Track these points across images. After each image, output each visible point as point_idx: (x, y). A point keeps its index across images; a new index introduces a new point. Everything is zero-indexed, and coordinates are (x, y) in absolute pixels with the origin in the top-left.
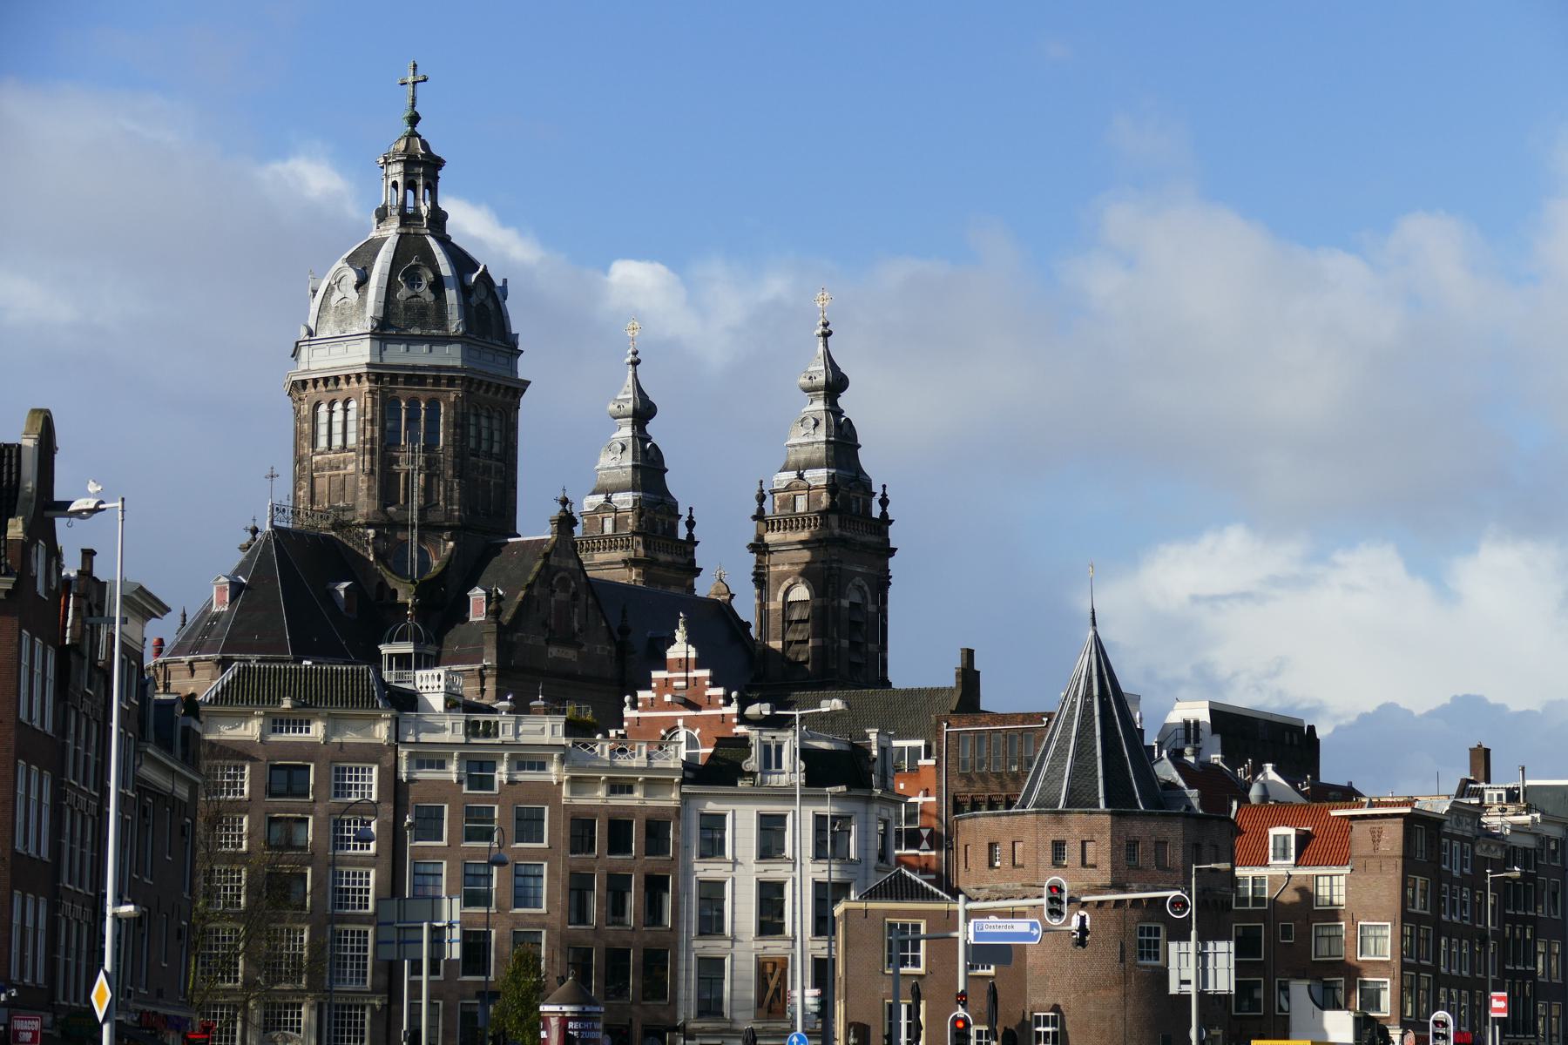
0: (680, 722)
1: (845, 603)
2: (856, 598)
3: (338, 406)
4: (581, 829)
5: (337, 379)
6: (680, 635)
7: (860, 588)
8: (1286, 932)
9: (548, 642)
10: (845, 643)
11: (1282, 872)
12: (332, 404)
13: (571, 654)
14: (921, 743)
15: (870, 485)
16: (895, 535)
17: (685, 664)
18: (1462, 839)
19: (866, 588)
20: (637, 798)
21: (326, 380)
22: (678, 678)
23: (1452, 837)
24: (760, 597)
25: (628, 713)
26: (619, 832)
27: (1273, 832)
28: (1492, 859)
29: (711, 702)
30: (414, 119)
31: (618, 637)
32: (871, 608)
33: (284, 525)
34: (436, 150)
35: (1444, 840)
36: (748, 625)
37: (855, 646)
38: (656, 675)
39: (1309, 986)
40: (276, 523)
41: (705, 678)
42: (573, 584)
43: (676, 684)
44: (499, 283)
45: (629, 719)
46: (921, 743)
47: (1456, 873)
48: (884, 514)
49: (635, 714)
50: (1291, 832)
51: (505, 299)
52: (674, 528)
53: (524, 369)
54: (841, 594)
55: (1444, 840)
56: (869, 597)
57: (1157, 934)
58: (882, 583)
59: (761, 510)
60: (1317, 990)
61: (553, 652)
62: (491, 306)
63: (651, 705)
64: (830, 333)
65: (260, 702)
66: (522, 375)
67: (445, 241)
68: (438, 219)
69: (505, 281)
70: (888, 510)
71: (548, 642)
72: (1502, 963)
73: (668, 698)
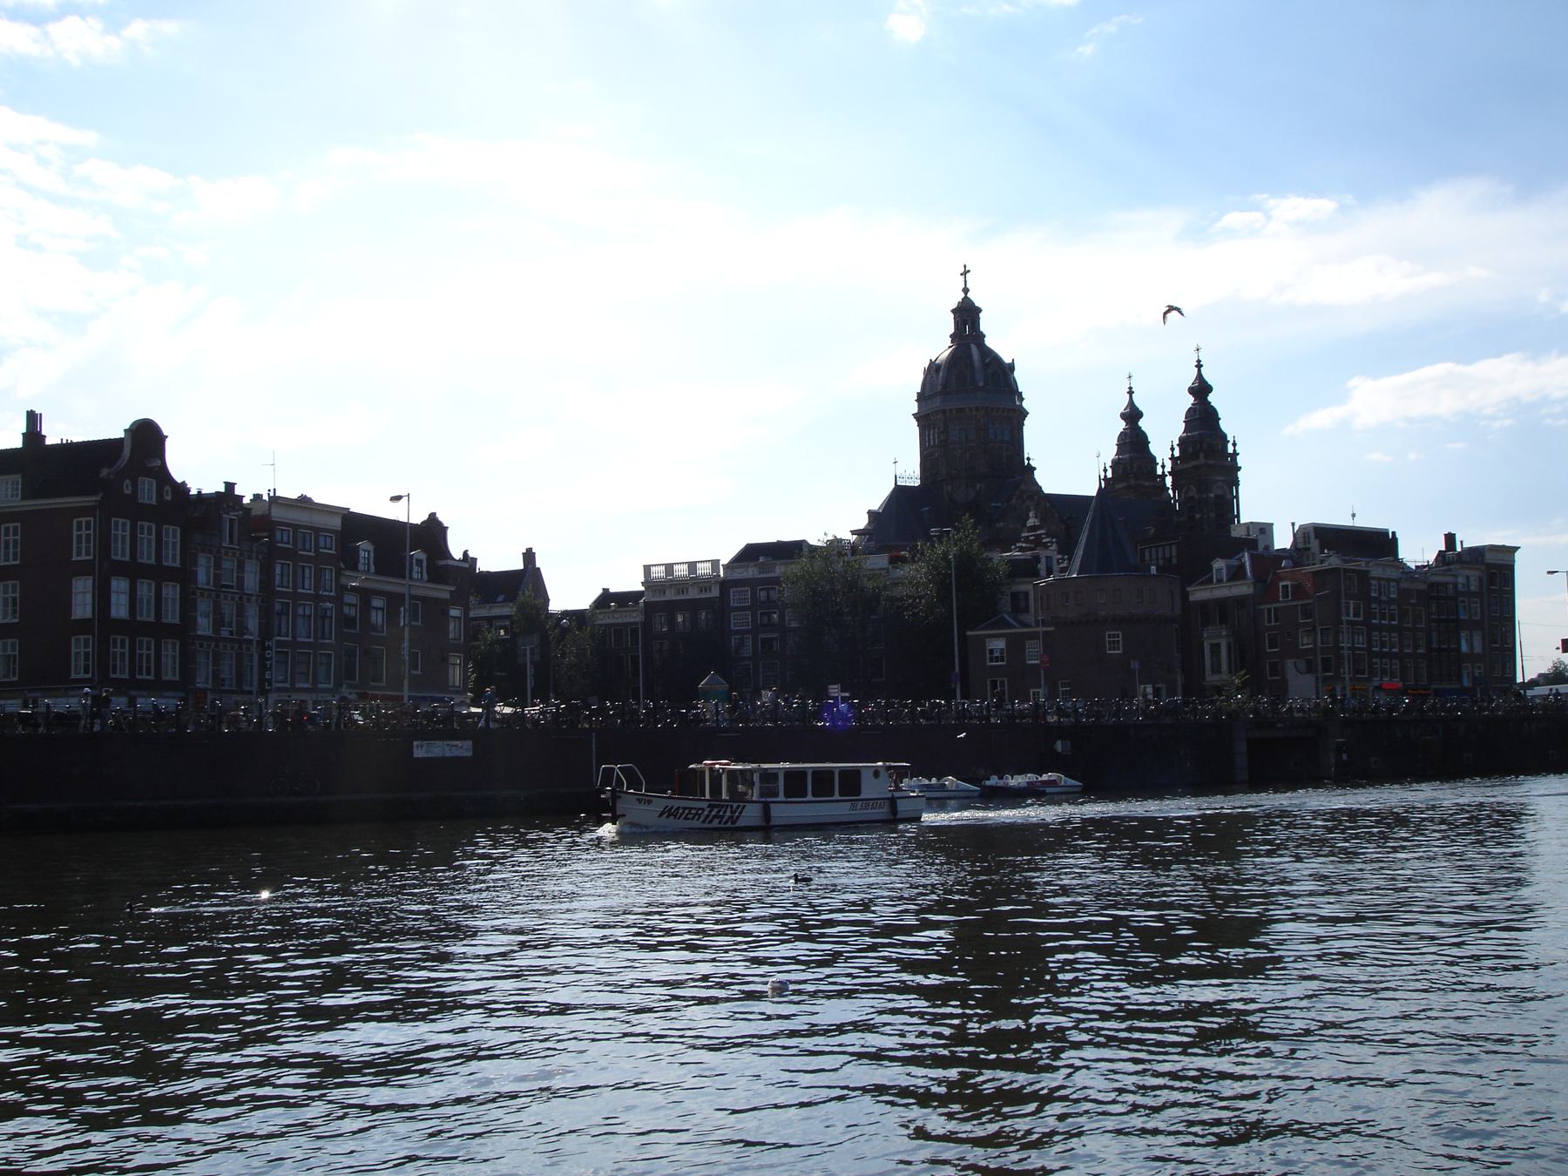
1: (1212, 495)
2: (1220, 492)
5: (928, 414)
16: (1240, 461)
17: (1034, 528)
27: (1281, 584)
28: (1418, 590)
30: (966, 290)
32: (1229, 496)
33: (912, 484)
39: (1295, 663)
40: (899, 484)
41: (1044, 534)
42: (1036, 497)
48: (1235, 450)
50: (1289, 583)
55: (1374, 582)
57: (1118, 637)
58: (1236, 483)
60: (1302, 665)
64: (1202, 366)
70: (1236, 448)
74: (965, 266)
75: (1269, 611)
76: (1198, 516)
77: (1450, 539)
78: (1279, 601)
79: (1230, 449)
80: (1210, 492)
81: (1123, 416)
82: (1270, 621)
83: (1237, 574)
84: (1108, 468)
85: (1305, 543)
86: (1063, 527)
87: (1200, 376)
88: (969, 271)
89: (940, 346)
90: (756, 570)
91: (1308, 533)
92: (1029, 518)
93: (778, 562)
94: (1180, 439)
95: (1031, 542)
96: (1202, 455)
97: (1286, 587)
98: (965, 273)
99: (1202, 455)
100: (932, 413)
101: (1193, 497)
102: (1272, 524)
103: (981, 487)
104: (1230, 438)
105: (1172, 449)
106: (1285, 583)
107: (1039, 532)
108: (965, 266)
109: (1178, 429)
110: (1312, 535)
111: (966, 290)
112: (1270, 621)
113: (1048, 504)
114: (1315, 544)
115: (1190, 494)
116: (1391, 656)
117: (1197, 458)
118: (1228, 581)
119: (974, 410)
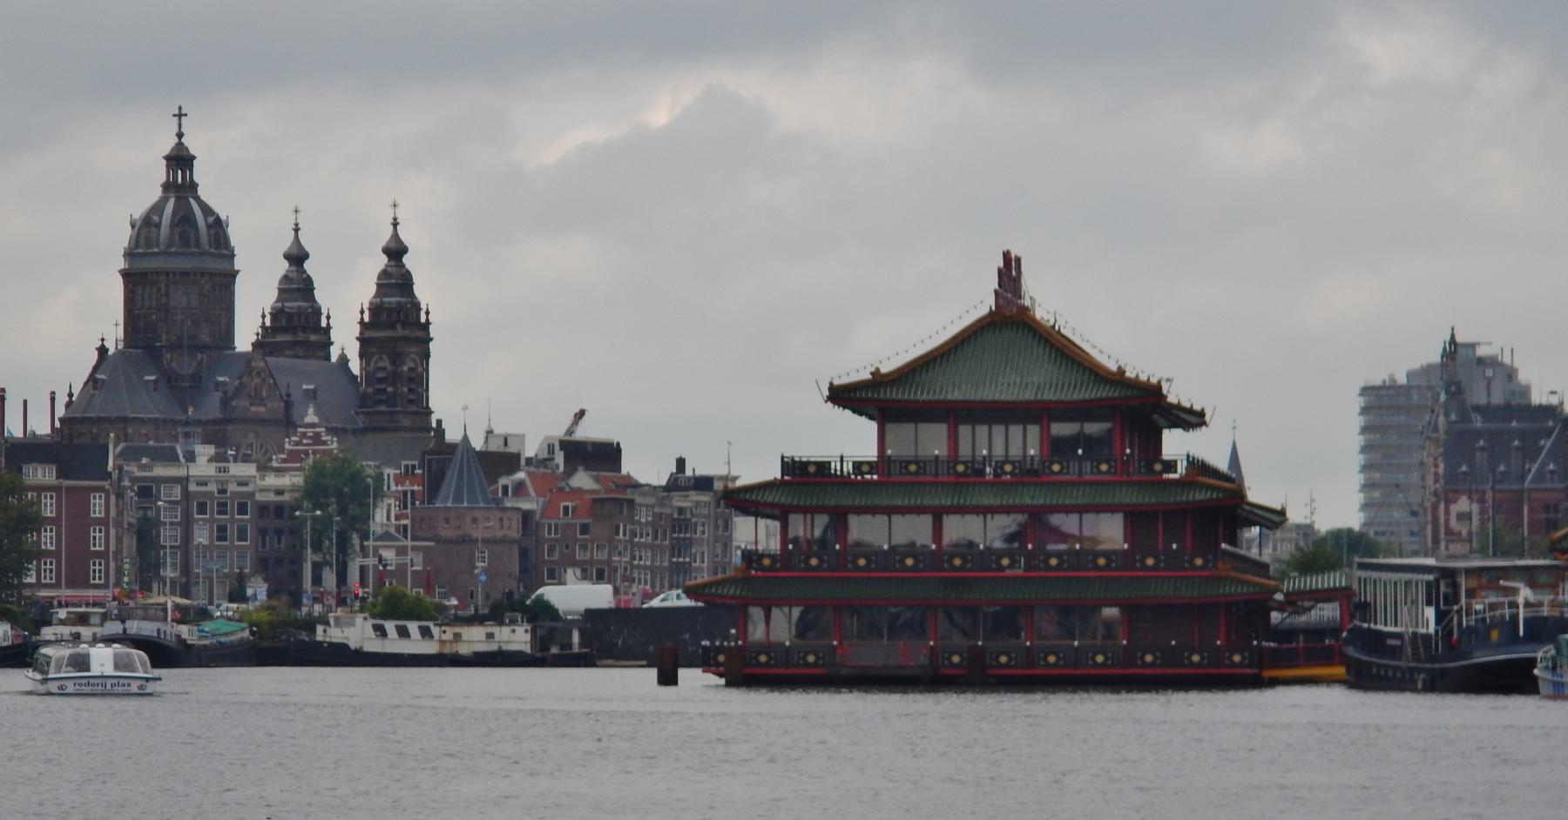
0: (310, 452)
1: (405, 368)
4: (263, 508)
5: (146, 274)
6: (311, 411)
7: (414, 360)
8: (567, 547)
10: (406, 389)
11: (565, 521)
13: (262, 409)
14: (416, 463)
15: (420, 304)
17: (312, 425)
18: (647, 506)
19: (417, 359)
20: (286, 497)
21: (141, 273)
22: (310, 431)
23: (640, 505)
24: (361, 364)
25: (287, 446)
26: (279, 510)
29: (324, 443)
30: (180, 135)
31: (285, 398)
32: (420, 369)
34: (192, 152)
35: (636, 507)
36: (357, 376)
37: (411, 390)
38: (299, 430)
43: (309, 434)
44: (223, 217)
45: (287, 450)
47: (643, 520)
49: (291, 448)
50: (570, 504)
51: (227, 226)
53: (238, 264)
54: (403, 364)
56: (419, 363)
58: (427, 356)
59: (362, 319)
60: (578, 572)
61: (254, 409)
62: (221, 232)
63: (297, 443)
66: (236, 268)
67: (198, 199)
68: (193, 187)
69: (228, 217)
71: (251, 404)
73: (304, 441)
74: (180, 108)
75: (550, 526)
76: (390, 389)
77: (681, 463)
78: (559, 519)
79: (423, 320)
80: (405, 365)
81: (287, 257)
82: (550, 533)
84: (266, 313)
85: (549, 453)
86: (283, 404)
87: (395, 235)
88: (186, 115)
91: (553, 445)
93: (158, 464)
94: (371, 303)
95: (310, 438)
96: (399, 326)
97: (566, 508)
98: (180, 115)
99: (399, 326)
100: (152, 273)
101: (384, 369)
102: (524, 436)
103: (202, 359)
104: (423, 306)
105: (362, 312)
106: (566, 504)
107: (318, 430)
108: (180, 108)
109: (366, 291)
110: (557, 447)
111: (180, 135)
112: (550, 533)
113: (272, 381)
114: (559, 458)
115: (381, 364)
116: (645, 568)
117: (395, 328)
119: (199, 274)
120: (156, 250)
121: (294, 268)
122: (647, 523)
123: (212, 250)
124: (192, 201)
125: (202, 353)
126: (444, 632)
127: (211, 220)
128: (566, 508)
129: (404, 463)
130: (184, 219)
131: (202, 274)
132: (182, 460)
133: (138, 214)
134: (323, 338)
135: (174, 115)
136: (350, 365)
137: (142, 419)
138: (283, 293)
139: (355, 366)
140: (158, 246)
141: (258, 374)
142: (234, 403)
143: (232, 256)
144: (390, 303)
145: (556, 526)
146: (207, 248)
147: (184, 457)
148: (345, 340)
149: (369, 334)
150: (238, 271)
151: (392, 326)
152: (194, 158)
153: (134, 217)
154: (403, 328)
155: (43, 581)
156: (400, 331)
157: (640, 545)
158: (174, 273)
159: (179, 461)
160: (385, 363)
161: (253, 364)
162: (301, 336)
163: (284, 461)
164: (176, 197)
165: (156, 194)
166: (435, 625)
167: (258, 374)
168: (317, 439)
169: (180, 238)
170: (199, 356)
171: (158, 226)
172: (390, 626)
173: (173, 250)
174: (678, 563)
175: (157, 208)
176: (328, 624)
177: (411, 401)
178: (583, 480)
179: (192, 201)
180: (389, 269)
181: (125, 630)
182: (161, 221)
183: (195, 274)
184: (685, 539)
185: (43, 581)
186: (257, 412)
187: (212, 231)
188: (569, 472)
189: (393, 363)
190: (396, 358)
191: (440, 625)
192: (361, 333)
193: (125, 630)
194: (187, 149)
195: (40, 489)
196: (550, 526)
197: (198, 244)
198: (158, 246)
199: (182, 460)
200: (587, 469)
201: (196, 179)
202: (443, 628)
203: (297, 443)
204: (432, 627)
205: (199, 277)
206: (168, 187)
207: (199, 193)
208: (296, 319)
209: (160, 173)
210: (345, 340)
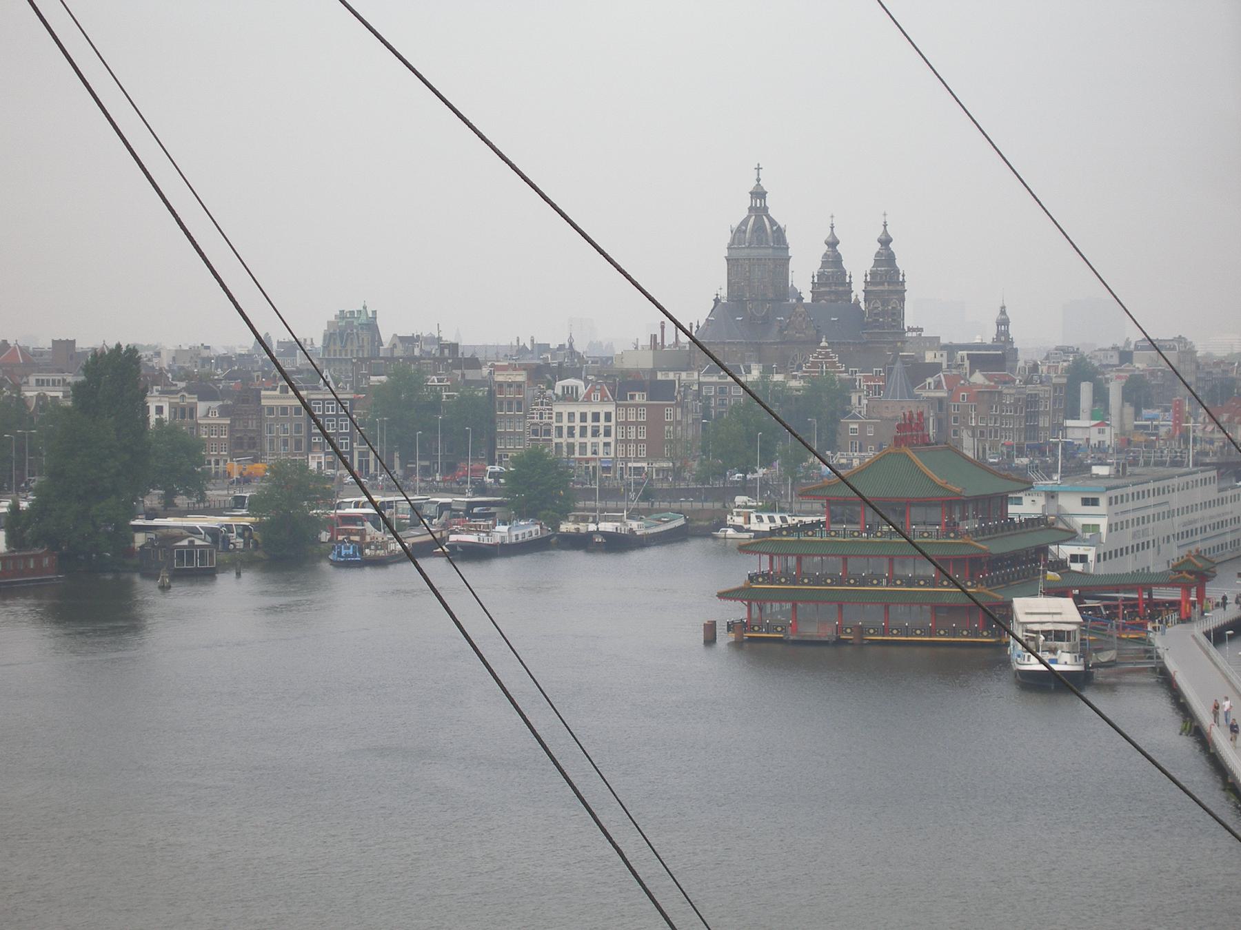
1: (890, 308)
2: (894, 306)
3: (739, 266)
5: (738, 259)
8: (964, 418)
9: (796, 333)
10: (890, 320)
12: (738, 265)
14: (881, 369)
18: (1010, 394)
21: (735, 259)
25: (811, 359)
29: (831, 358)
30: (758, 180)
34: (765, 189)
46: (881, 369)
50: (965, 394)
52: (845, 279)
58: (903, 300)
60: (970, 433)
61: (797, 335)
63: (817, 358)
65: (717, 373)
68: (765, 209)
70: (905, 278)
71: (796, 333)
72: (1025, 423)
74: (759, 165)
76: (881, 320)
79: (901, 280)
82: (954, 410)
83: (938, 386)
86: (815, 331)
89: (739, 211)
90: (717, 378)
92: (822, 342)
96: (886, 284)
97: (963, 396)
98: (759, 169)
99: (886, 284)
104: (901, 272)
105: (866, 276)
107: (828, 350)
108: (759, 165)
109: (869, 265)
111: (758, 180)
114: (967, 363)
116: (1009, 429)
117: (883, 285)
118: (935, 389)
120: (743, 246)
121: (830, 249)
122: (1010, 404)
123: (776, 246)
124: (764, 217)
125: (769, 303)
126: (794, 520)
127: (775, 228)
128: (963, 396)
129: (874, 369)
130: (759, 228)
131: (769, 259)
132: (744, 373)
133: (735, 225)
134: (848, 289)
135: (756, 169)
136: (861, 304)
137: (734, 343)
138: (825, 264)
139: (862, 305)
140: (744, 244)
141: (800, 315)
142: (786, 332)
143: (788, 248)
144: (881, 271)
145: (958, 406)
146: (772, 244)
147: (745, 371)
148: (858, 291)
149: (870, 288)
150: (791, 257)
151: (882, 284)
152: (766, 193)
153: (733, 226)
154: (888, 285)
155: (639, 456)
156: (886, 287)
157: (1006, 417)
158: (753, 259)
159: (742, 373)
160: (879, 304)
161: (797, 310)
162: (833, 288)
163: (809, 367)
164: (756, 216)
165: (745, 213)
166: (789, 516)
167: (800, 315)
168: (827, 356)
169: (757, 239)
170: (768, 305)
171: (745, 232)
172: (765, 516)
173: (753, 246)
174: (1030, 425)
175: (745, 222)
176: (732, 514)
177: (893, 326)
178: (978, 378)
179: (764, 217)
180: (881, 251)
181: (598, 529)
182: (746, 229)
183: (766, 259)
184: (1034, 412)
185: (639, 456)
186: (799, 337)
187: (775, 235)
188: (972, 373)
189: (882, 305)
190: (885, 303)
191: (792, 516)
192: (865, 288)
193: (598, 529)
194: (762, 188)
195: (637, 406)
196: (954, 406)
197: (767, 240)
198: (744, 244)
199: (744, 373)
200: (981, 371)
201: (767, 205)
202: (793, 518)
203: (817, 358)
204: (787, 517)
205: (767, 261)
206: (751, 209)
207: (769, 212)
208: (831, 278)
209: (747, 202)
210: (858, 291)
